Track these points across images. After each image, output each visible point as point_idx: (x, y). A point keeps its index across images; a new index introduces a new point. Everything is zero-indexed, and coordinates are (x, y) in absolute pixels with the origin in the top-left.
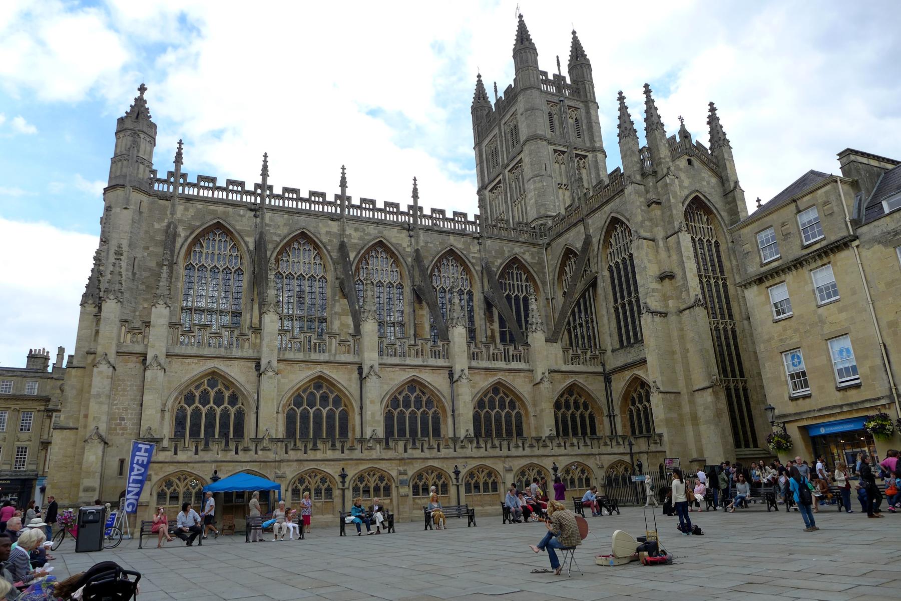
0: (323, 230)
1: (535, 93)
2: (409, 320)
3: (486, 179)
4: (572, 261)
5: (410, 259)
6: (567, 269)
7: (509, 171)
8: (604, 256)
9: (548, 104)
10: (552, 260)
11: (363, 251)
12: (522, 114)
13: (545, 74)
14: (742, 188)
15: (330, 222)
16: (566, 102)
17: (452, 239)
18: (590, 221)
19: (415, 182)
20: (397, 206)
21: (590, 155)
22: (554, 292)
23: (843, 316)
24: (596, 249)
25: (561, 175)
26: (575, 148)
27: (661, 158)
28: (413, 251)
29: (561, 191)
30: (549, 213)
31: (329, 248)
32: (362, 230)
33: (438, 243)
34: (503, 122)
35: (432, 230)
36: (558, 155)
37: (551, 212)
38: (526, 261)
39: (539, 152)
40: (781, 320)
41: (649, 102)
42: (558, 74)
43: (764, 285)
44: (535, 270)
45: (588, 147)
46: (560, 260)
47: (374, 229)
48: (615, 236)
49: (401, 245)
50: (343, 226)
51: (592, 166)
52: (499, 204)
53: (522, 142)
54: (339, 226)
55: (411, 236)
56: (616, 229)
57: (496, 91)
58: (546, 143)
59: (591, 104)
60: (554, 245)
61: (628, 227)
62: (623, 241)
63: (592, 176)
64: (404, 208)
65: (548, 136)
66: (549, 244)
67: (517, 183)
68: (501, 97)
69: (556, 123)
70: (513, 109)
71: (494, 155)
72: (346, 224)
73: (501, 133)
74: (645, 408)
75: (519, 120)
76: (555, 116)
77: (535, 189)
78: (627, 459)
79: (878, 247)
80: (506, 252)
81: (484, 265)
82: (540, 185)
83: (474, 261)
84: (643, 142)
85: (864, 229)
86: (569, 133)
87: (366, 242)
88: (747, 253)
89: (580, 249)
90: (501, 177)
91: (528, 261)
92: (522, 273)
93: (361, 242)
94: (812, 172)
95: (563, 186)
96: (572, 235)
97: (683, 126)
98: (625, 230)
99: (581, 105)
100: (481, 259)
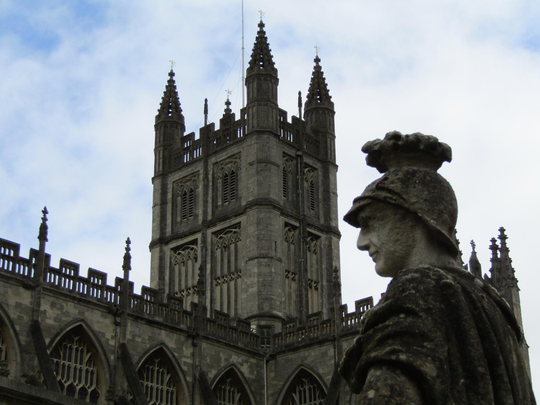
0: (12, 301)
1: (273, 141)
3: (169, 230)
4: (307, 388)
5: (112, 357)
6: (296, 398)
7: (213, 233)
9: (284, 157)
10: (275, 378)
11: (58, 338)
12: (251, 164)
13: (284, 114)
14: (527, 343)
15: (22, 290)
16: (304, 157)
17: (164, 336)
19: (128, 246)
20: (103, 276)
21: (323, 236)
25: (288, 258)
26: (309, 225)
28: (117, 345)
29: (287, 281)
30: (275, 312)
31: (18, 328)
32: (59, 306)
33: (147, 338)
34: (213, 160)
35: (142, 319)
36: (289, 230)
37: (277, 310)
38: (243, 376)
39: (271, 224)
42: (298, 117)
44: (253, 389)
45: (322, 225)
46: (288, 383)
47: (75, 307)
49: (103, 335)
50: (39, 298)
51: (324, 252)
52: (187, 272)
53: (244, 203)
54: (32, 297)
55: (117, 324)
57: (206, 112)
58: (278, 213)
59: (331, 168)
60: (281, 359)
63: (324, 266)
64: (111, 282)
65: (282, 203)
66: (273, 357)
67: (226, 254)
68: (213, 125)
69: (290, 184)
70: (234, 150)
71: (188, 198)
72: (42, 296)
75: (244, 169)
76: (289, 174)
77: (259, 275)
80: (223, 359)
81: (197, 375)
83: (185, 368)
86: (303, 203)
87: (63, 325)
90: (198, 236)
91: (247, 375)
92: (236, 391)
93: (56, 324)
95: (290, 275)
96: (313, 354)
97: (474, 253)
99: (318, 165)
100: (194, 367)
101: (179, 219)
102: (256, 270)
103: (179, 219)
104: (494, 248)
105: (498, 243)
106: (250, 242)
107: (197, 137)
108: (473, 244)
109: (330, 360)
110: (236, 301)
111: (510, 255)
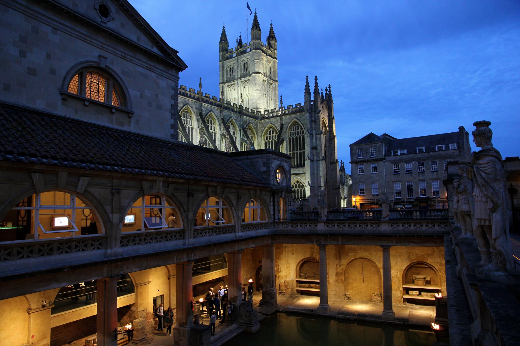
2: (219, 147)
8: (288, 133)
10: (262, 127)
18: (284, 119)
22: (261, 140)
23: (378, 177)
24: (285, 130)
27: (318, 106)
40: (360, 175)
41: (316, 83)
43: (357, 164)
48: (294, 127)
56: (294, 125)
61: (300, 126)
62: (297, 130)
73: (238, 62)
74: (298, 190)
78: (299, 206)
79: (389, 163)
82: (259, 95)
84: (312, 99)
85: (387, 157)
88: (354, 154)
89: (279, 128)
90: (236, 82)
94: (372, 134)
97: (322, 93)
98: (299, 126)
101: (228, 76)
102: (255, 94)
103: (228, 76)
104: (326, 90)
105: (328, 89)
107: (234, 50)
108: (322, 90)
109: (279, 122)
110: (248, 103)
111: (332, 93)
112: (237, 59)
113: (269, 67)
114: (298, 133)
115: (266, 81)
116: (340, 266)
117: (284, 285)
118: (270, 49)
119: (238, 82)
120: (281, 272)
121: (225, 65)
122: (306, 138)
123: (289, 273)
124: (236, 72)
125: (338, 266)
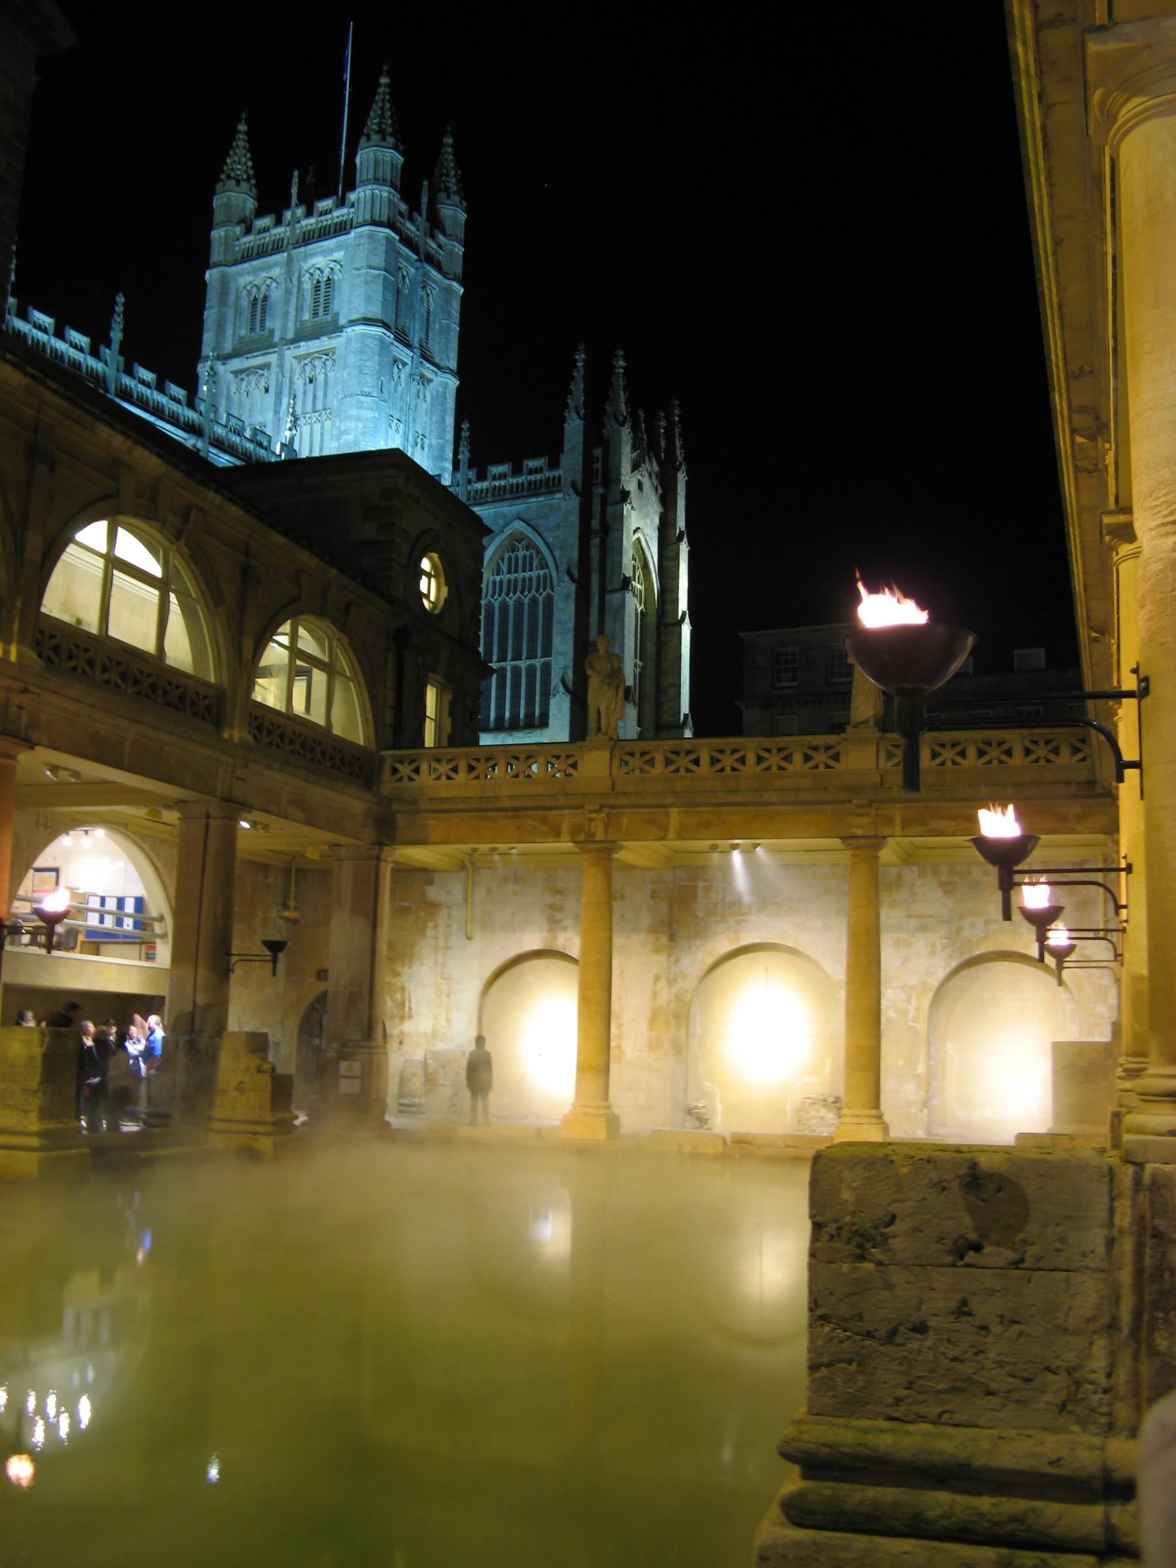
39: (379, 355)
61: (539, 552)
90: (272, 358)
98: (531, 557)
102: (354, 412)
106: (349, 374)
112: (290, 261)
113: (424, 310)
114: (527, 585)
115: (404, 364)
116: (671, 982)
117: (420, 1072)
118: (433, 237)
119: (281, 358)
120: (411, 1017)
121: (233, 284)
122: (558, 604)
123: (448, 1020)
124: (280, 314)
125: (662, 983)
